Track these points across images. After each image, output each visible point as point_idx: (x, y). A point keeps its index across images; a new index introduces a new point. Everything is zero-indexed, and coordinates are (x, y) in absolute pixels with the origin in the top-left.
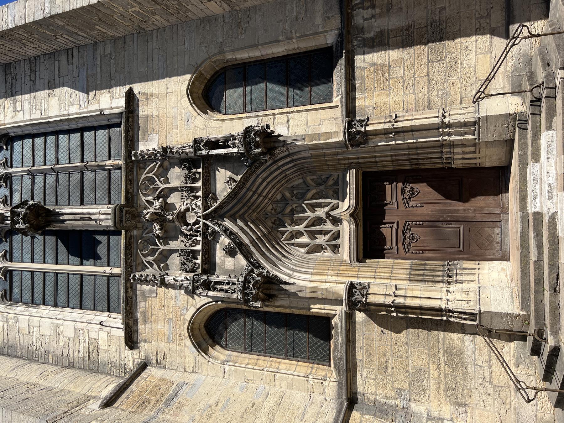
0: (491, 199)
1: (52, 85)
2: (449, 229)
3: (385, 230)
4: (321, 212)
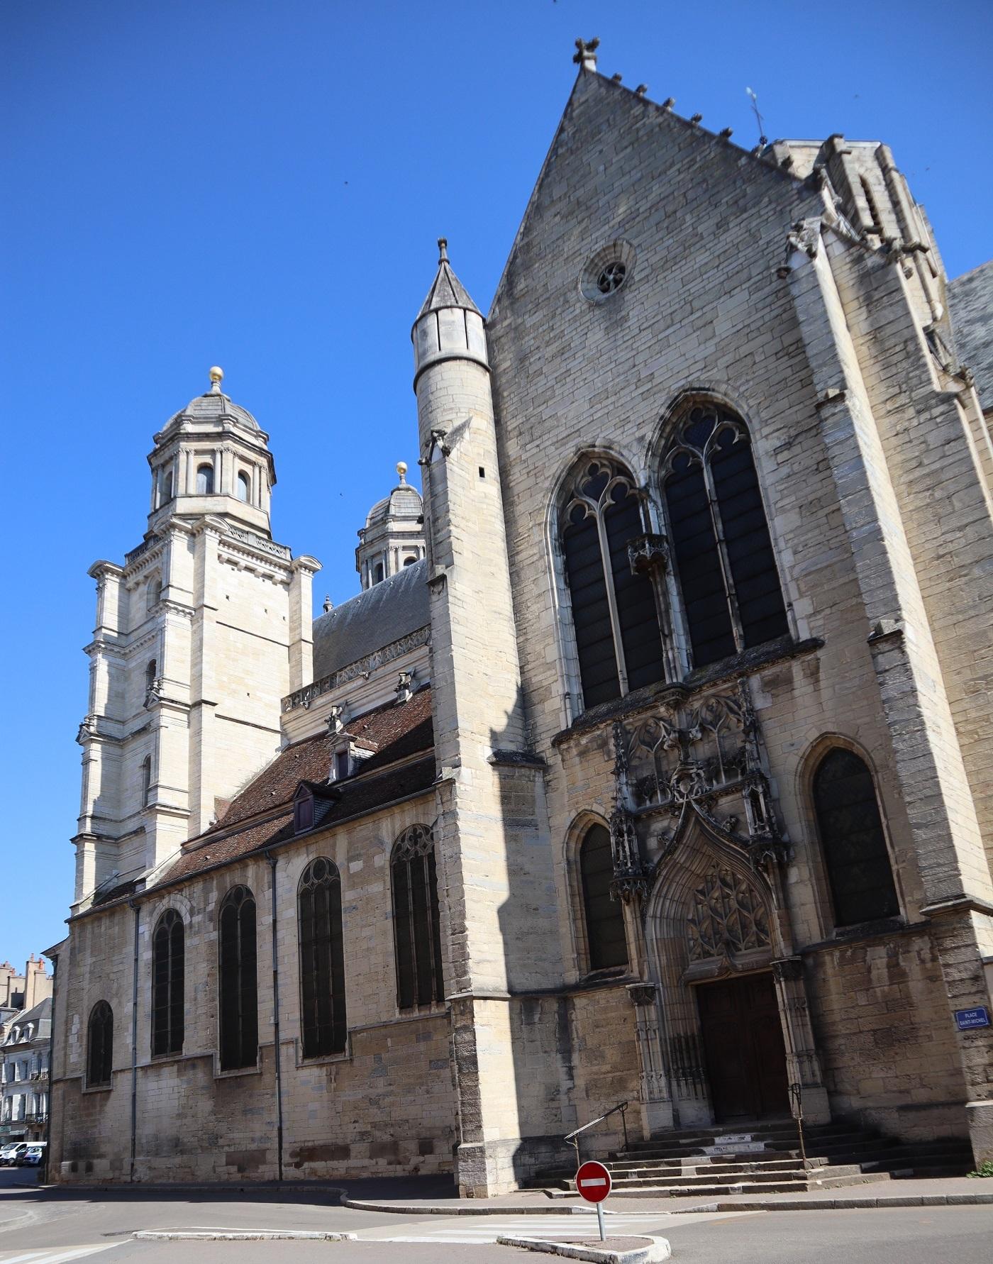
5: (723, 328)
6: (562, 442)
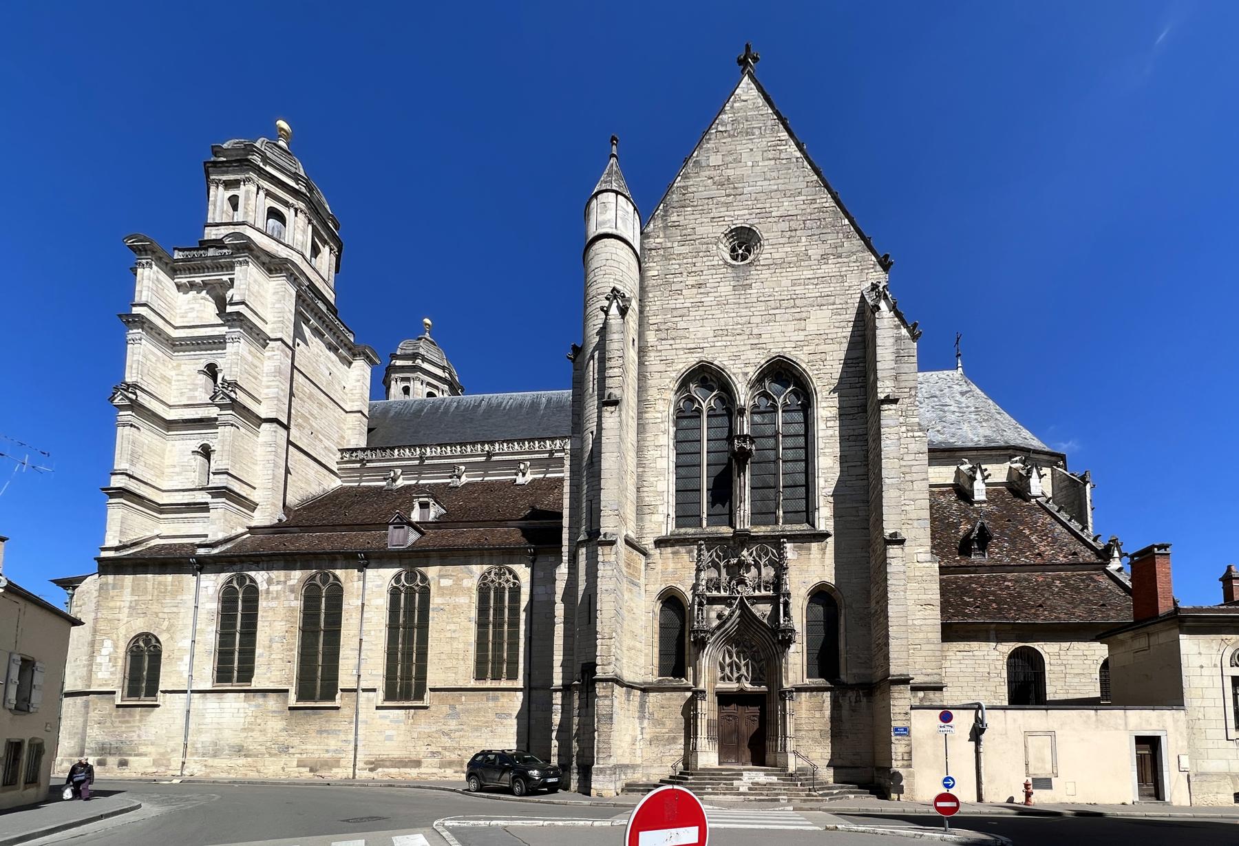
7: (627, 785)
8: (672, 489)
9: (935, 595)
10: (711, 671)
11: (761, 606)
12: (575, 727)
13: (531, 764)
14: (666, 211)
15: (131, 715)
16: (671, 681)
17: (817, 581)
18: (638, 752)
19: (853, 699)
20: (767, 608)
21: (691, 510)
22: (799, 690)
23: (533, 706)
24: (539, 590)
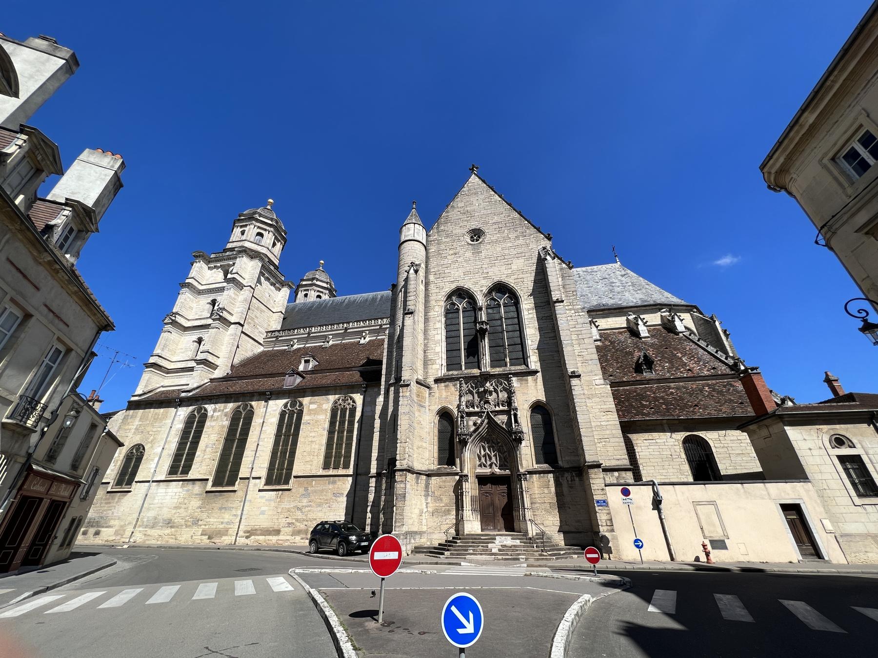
0: (503, 525)
1: (540, 329)
2: (491, 510)
3: (489, 485)
4: (494, 459)
5: (514, 267)
6: (452, 282)
7: (415, 548)
8: (444, 350)
9: (611, 404)
10: (473, 461)
11: (500, 417)
12: (382, 503)
13: (351, 531)
14: (438, 226)
15: (113, 499)
16: (446, 468)
17: (534, 399)
18: (424, 521)
19: (569, 479)
20: (504, 418)
21: (455, 361)
22: (531, 473)
23: (358, 487)
24: (368, 409)
